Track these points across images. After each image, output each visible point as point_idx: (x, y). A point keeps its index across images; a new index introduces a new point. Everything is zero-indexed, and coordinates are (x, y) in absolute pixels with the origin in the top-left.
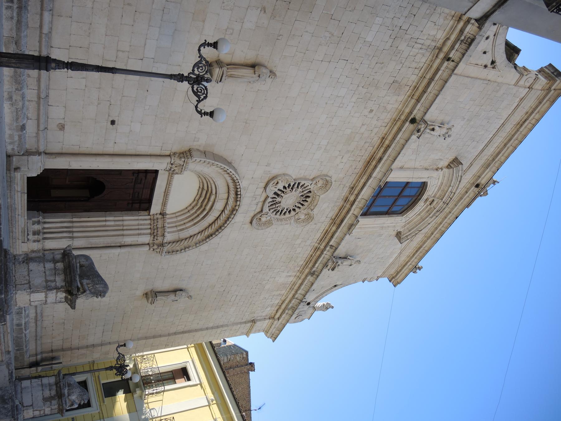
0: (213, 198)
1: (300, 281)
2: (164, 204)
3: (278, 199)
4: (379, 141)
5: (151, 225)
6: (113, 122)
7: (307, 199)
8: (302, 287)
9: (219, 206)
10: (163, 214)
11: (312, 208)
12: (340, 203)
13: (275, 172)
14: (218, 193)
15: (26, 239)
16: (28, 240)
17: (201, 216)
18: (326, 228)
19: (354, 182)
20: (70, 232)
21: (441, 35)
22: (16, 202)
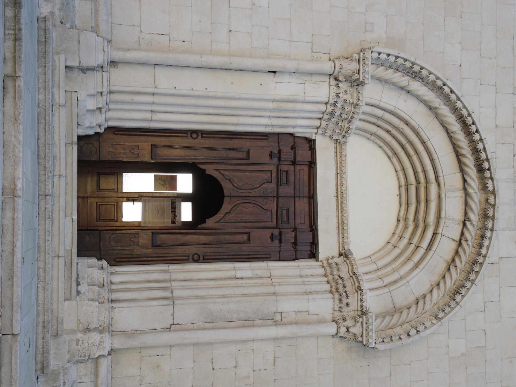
0: (433, 189)
2: (342, 229)
5: (325, 276)
10: (345, 254)
14: (440, 174)
15: (74, 292)
16: (78, 293)
17: (425, 244)
20: (164, 289)
22: (56, 138)
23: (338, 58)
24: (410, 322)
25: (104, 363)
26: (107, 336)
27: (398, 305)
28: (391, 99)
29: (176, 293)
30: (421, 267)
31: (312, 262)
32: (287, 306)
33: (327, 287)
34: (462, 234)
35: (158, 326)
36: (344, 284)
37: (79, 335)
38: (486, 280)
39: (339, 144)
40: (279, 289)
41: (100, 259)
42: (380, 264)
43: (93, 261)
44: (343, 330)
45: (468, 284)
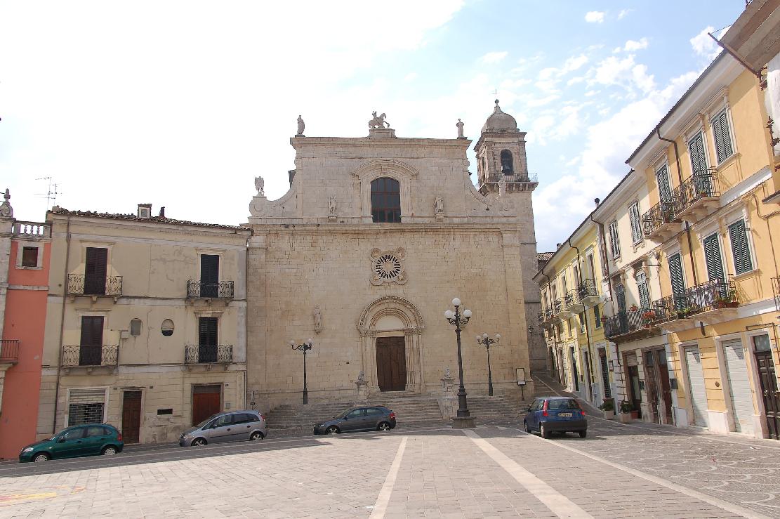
12: (388, 235)
13: (368, 283)
21: (287, 237)
28: (369, 322)
39: (379, 332)
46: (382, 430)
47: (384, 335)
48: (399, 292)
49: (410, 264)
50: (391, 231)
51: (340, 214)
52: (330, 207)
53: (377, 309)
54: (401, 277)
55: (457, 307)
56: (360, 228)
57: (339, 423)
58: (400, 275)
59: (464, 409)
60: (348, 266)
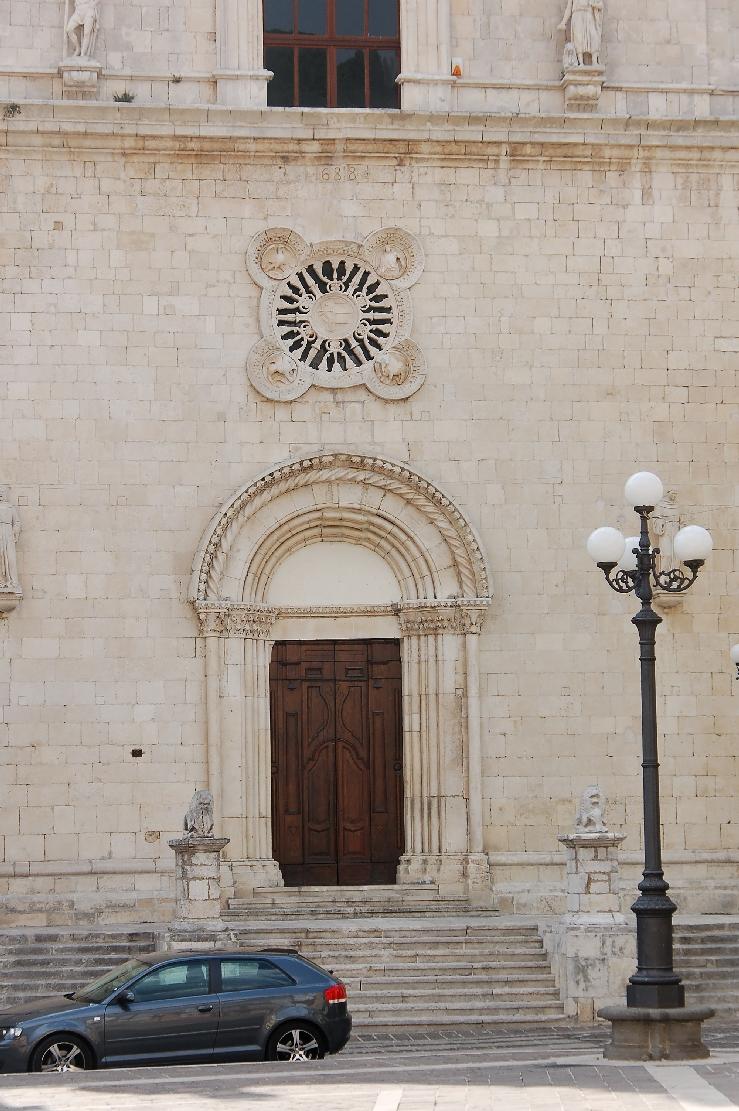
1: (659, 153)
2: (370, 613)
3: (335, 348)
4: (135, 159)
5: (419, 636)
6: (137, 753)
7: (335, 266)
8: (680, 142)
9: (349, 497)
10: (396, 611)
11: (355, 249)
15: (433, 886)
17: (389, 526)
18: (439, 164)
19: (267, 161)
23: (201, 631)
24: (466, 560)
25: (495, 857)
26: (472, 857)
27: (451, 563)
28: (239, 568)
29: (434, 792)
30: (412, 535)
31: (405, 646)
32: (449, 682)
33: (431, 639)
34: (380, 487)
35: (464, 810)
36: (428, 623)
37: (470, 881)
38: (423, 468)
39: (281, 614)
40: (432, 691)
41: (399, 862)
42: (407, 573)
43: (401, 868)
44: (474, 629)
45: (431, 490)
46: (285, 1056)
47: (308, 631)
48: (384, 435)
49: (431, 308)
50: (357, 150)
51: (114, 61)
52: (71, 25)
53: (280, 510)
54: (395, 366)
55: (644, 511)
56: (207, 131)
57: (96, 1018)
58: (387, 357)
59: (656, 975)
60: (151, 305)
